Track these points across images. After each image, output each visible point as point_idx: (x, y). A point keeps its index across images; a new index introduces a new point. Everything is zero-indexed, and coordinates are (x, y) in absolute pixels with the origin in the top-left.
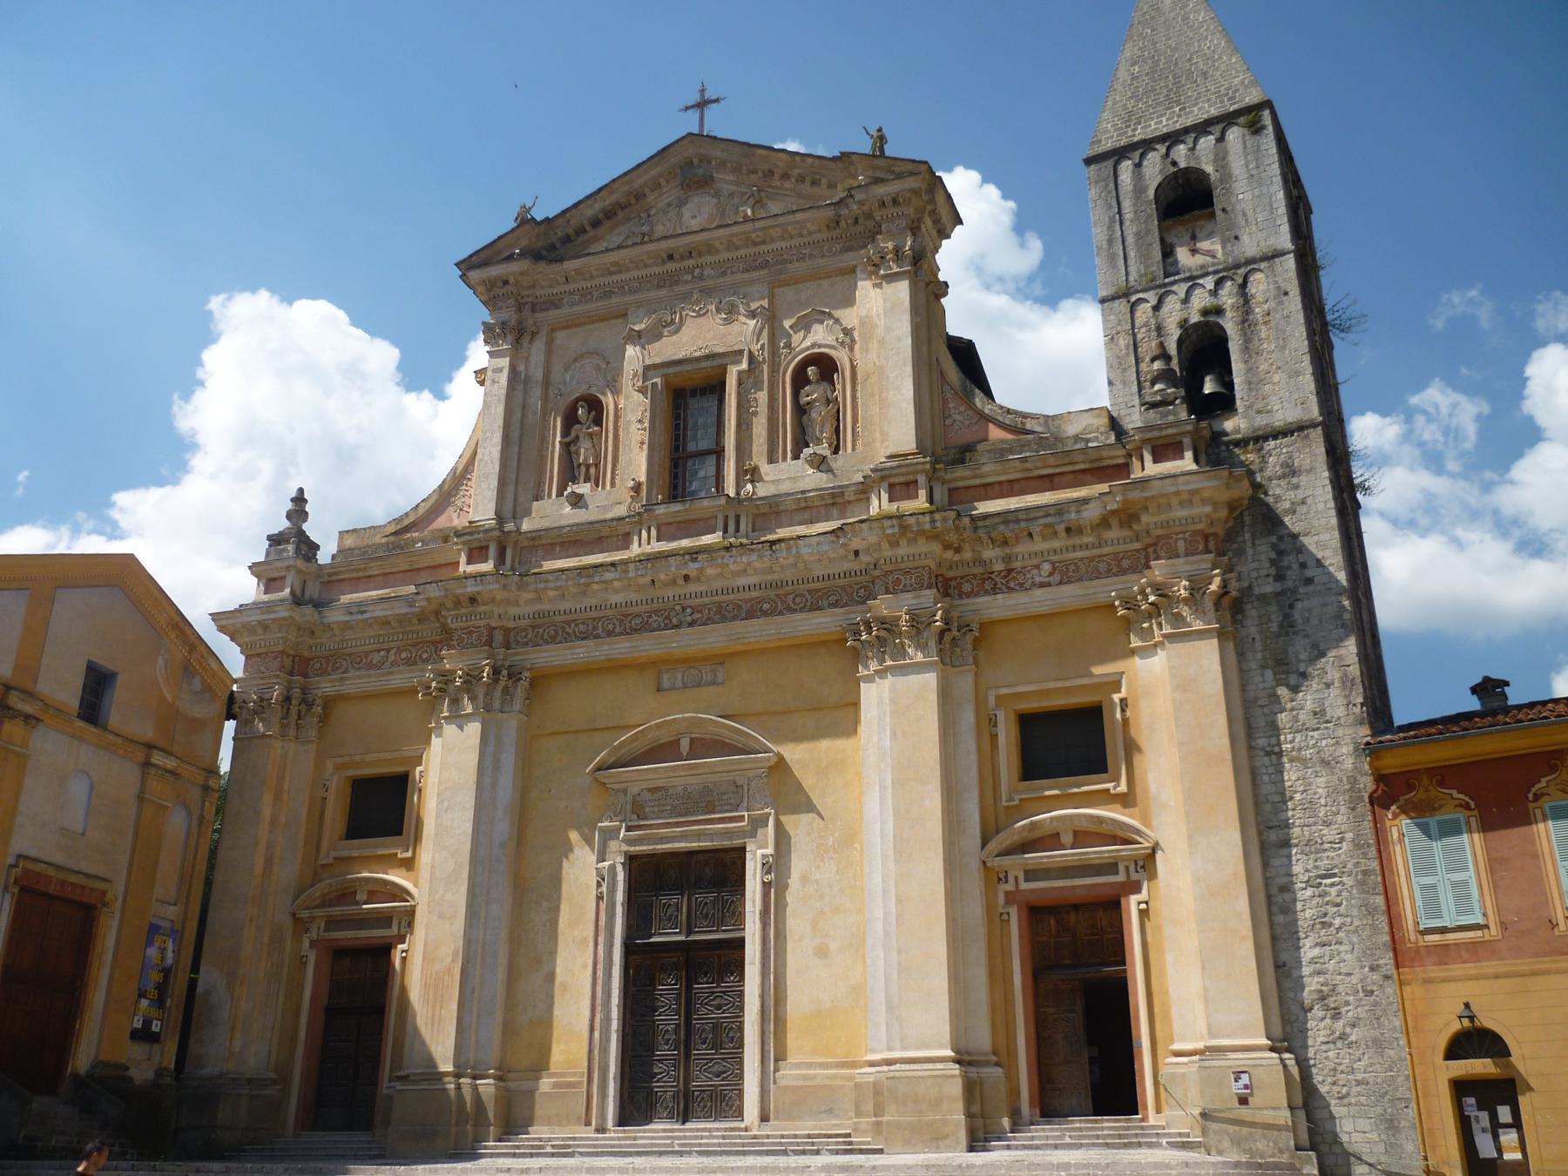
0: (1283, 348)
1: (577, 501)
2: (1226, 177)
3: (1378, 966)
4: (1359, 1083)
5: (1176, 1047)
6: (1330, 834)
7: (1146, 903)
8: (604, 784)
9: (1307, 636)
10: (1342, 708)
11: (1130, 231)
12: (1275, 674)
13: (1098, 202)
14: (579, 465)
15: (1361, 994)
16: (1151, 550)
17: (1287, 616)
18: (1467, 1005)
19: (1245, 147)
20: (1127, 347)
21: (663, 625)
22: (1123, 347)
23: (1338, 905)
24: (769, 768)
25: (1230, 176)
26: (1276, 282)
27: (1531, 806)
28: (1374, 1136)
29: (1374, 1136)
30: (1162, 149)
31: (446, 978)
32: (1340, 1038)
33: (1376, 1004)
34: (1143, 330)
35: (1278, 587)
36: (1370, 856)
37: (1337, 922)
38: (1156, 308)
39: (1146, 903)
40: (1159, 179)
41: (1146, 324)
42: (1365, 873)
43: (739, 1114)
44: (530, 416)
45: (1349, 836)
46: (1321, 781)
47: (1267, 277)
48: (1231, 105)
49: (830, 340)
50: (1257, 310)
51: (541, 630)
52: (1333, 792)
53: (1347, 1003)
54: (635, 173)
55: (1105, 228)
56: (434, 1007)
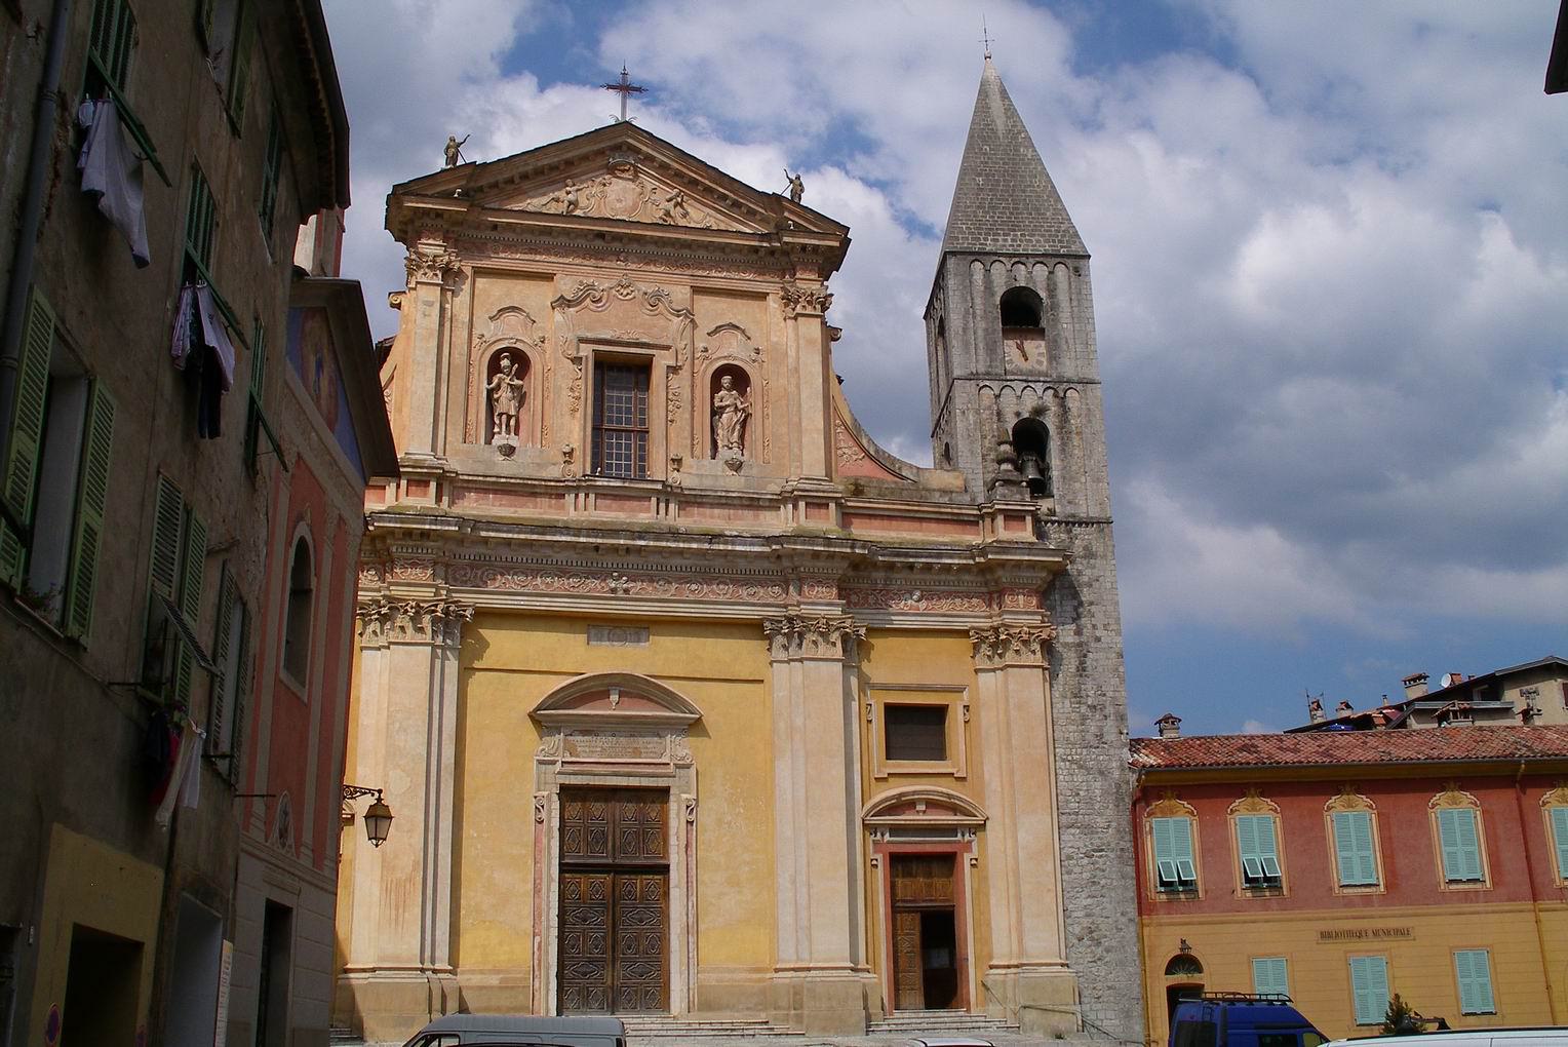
0: (1090, 457)
1: (509, 451)
2: (1054, 306)
3: (1127, 913)
4: (1109, 988)
5: (995, 962)
6: (1101, 821)
7: (976, 860)
8: (540, 722)
9: (1094, 680)
10: (1114, 735)
11: (982, 325)
12: (1071, 702)
13: (956, 293)
14: (500, 415)
15: (1115, 931)
16: (995, 596)
17: (1082, 663)
18: (1183, 942)
19: (1070, 288)
20: (975, 423)
21: (599, 587)
22: (971, 422)
23: (1104, 871)
24: (690, 725)
25: (1058, 306)
26: (1087, 404)
27: (1229, 817)
28: (1117, 1022)
29: (1117, 1022)
30: (1008, 263)
31: (408, 886)
32: (1099, 959)
33: (1123, 937)
34: (988, 412)
35: (1077, 640)
36: (1126, 839)
37: (1103, 882)
38: (997, 397)
39: (976, 860)
40: (1004, 289)
41: (990, 408)
42: (1122, 849)
43: (665, 1005)
44: (457, 356)
45: (1114, 824)
46: (1098, 784)
47: (1081, 398)
48: (1062, 247)
49: (742, 355)
50: (1072, 421)
51: (480, 573)
52: (1105, 793)
53: (1105, 936)
54: (569, 142)
55: (961, 317)
56: (397, 910)
